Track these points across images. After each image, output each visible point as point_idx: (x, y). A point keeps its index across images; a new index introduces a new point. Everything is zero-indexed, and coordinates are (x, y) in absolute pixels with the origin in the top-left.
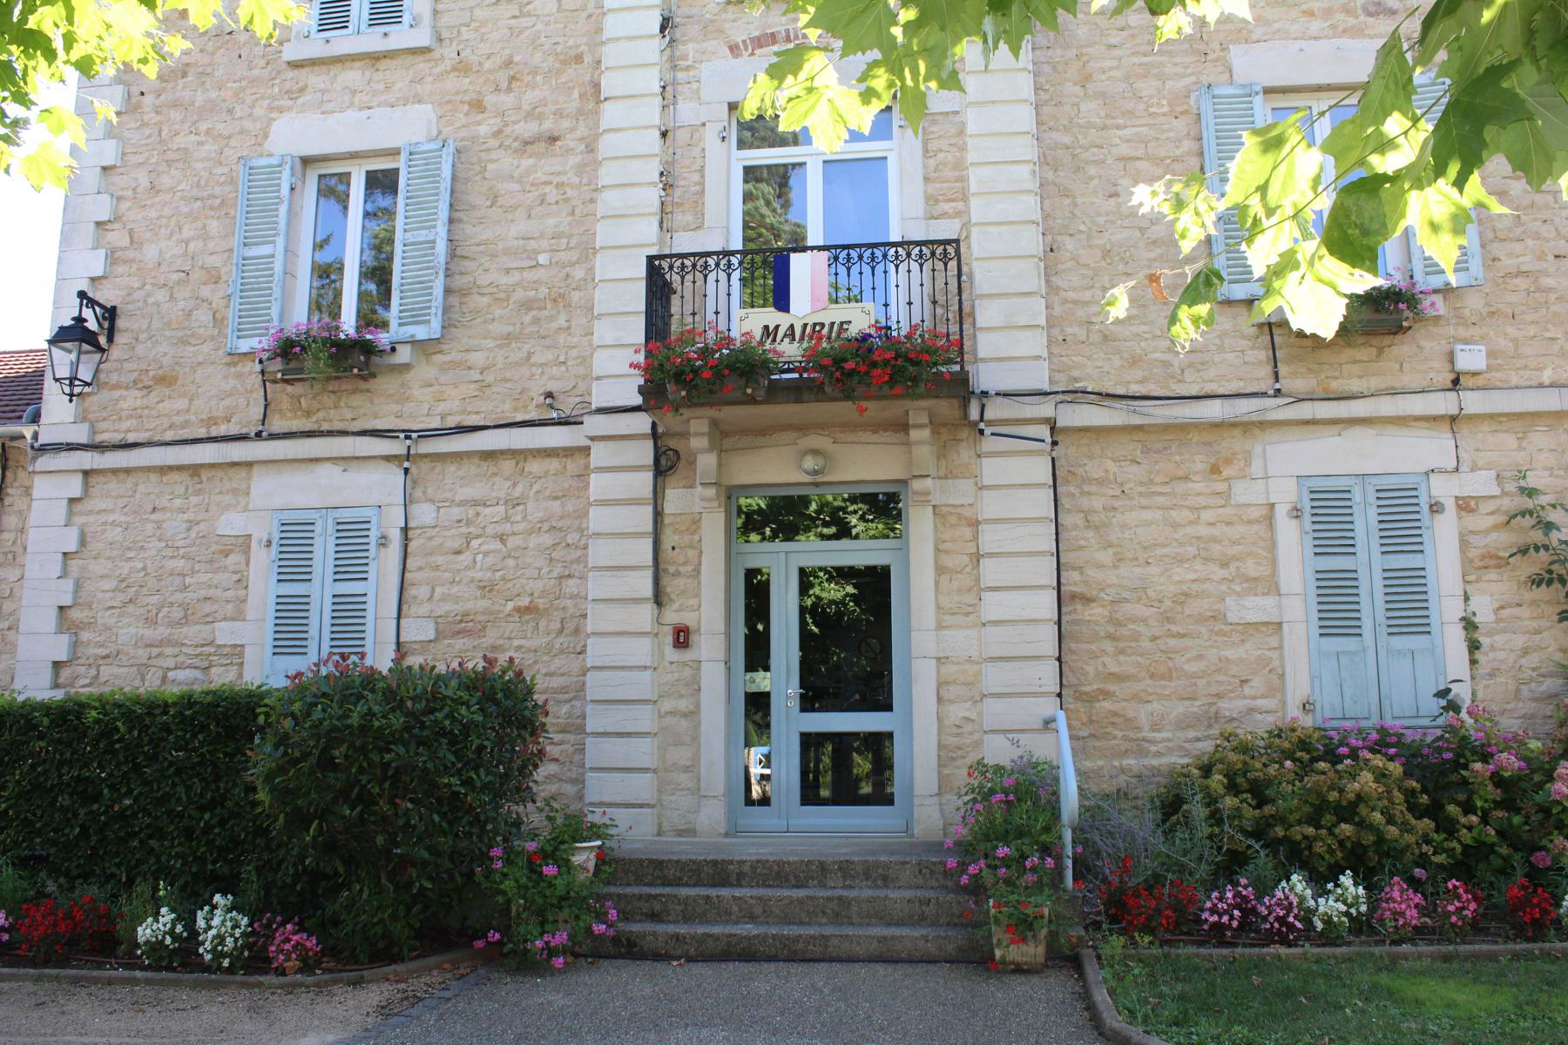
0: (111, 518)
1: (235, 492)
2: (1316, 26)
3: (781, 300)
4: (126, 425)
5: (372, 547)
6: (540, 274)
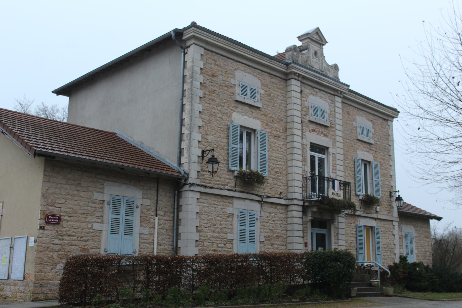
0: (205, 205)
1: (230, 203)
2: (365, 149)
3: (334, 189)
4: (207, 181)
5: (256, 220)
6: (278, 166)
